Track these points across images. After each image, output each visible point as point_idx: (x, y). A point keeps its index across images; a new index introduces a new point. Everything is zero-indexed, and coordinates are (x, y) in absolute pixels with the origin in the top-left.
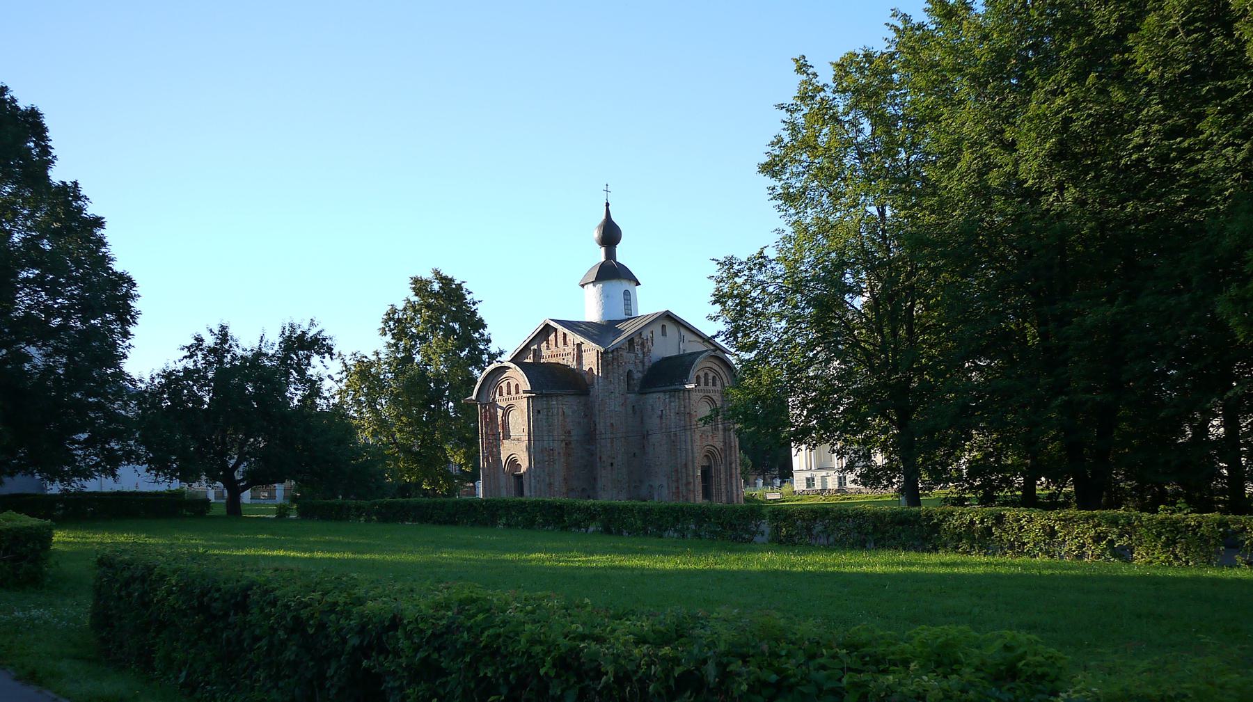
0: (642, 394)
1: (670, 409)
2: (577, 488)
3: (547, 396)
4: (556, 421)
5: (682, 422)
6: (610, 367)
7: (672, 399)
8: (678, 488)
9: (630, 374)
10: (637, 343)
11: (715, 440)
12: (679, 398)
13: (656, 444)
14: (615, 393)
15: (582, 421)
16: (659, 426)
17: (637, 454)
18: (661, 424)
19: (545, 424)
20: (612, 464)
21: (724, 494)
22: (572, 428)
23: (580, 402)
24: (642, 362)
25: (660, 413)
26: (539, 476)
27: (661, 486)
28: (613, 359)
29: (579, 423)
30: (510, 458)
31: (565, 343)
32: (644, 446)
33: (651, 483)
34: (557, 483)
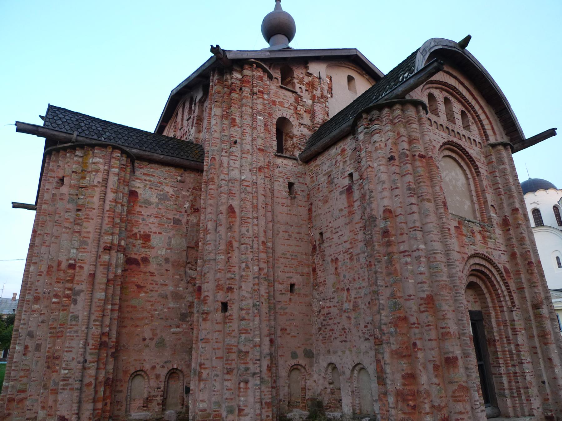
2: (154, 368)
4: (96, 199)
5: (409, 178)
6: (235, 95)
8: (411, 377)
9: (282, 123)
10: (301, 81)
11: (491, 243)
13: (340, 257)
14: (241, 144)
15: (184, 220)
16: (345, 212)
17: (296, 287)
21: (534, 391)
22: (154, 229)
23: (181, 182)
24: (312, 113)
25: (347, 182)
27: (359, 367)
29: (177, 222)
32: (314, 270)
33: (334, 359)
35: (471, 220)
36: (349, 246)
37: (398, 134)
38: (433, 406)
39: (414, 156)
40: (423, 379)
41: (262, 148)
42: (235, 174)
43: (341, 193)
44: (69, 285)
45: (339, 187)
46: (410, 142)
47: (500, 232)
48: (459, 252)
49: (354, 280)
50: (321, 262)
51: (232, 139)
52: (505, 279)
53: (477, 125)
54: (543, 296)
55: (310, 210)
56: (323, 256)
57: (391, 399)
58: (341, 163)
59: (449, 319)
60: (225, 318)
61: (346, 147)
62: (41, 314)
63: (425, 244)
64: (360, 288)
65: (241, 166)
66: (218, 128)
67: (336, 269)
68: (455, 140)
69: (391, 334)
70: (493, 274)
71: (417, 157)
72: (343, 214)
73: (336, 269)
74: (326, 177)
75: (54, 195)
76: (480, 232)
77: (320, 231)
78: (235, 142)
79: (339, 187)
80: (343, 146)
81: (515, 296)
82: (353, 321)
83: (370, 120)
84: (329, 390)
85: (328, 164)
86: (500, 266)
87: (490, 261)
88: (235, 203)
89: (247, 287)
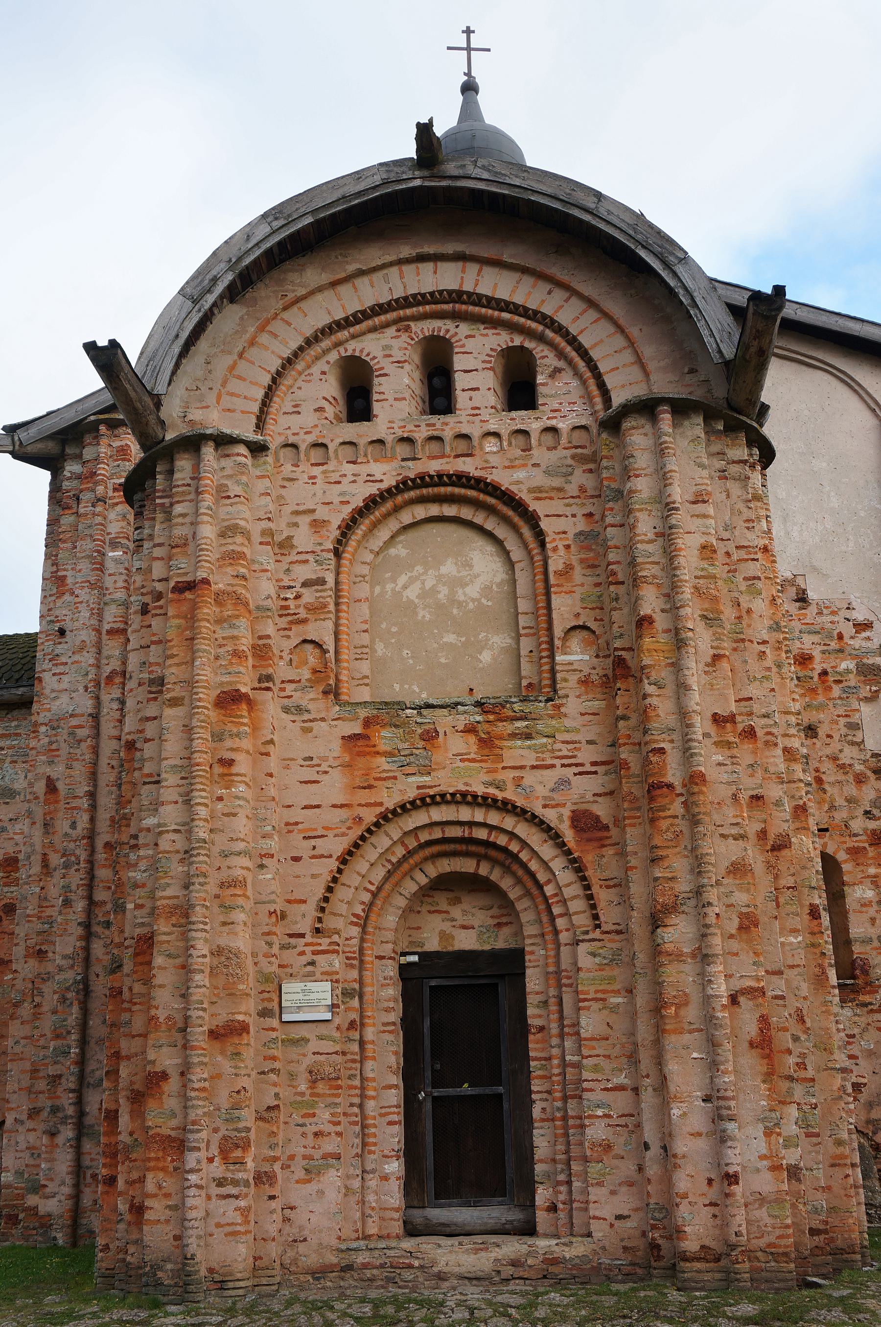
35: (431, 701)
41: (122, 626)
47: (596, 705)
48: (342, 806)
51: (56, 627)
52: (569, 852)
53: (577, 374)
54: (683, 886)
59: (160, 986)
68: (434, 467)
70: (524, 844)
76: (470, 729)
78: (62, 632)
81: (603, 896)
86: (550, 816)
87: (506, 807)
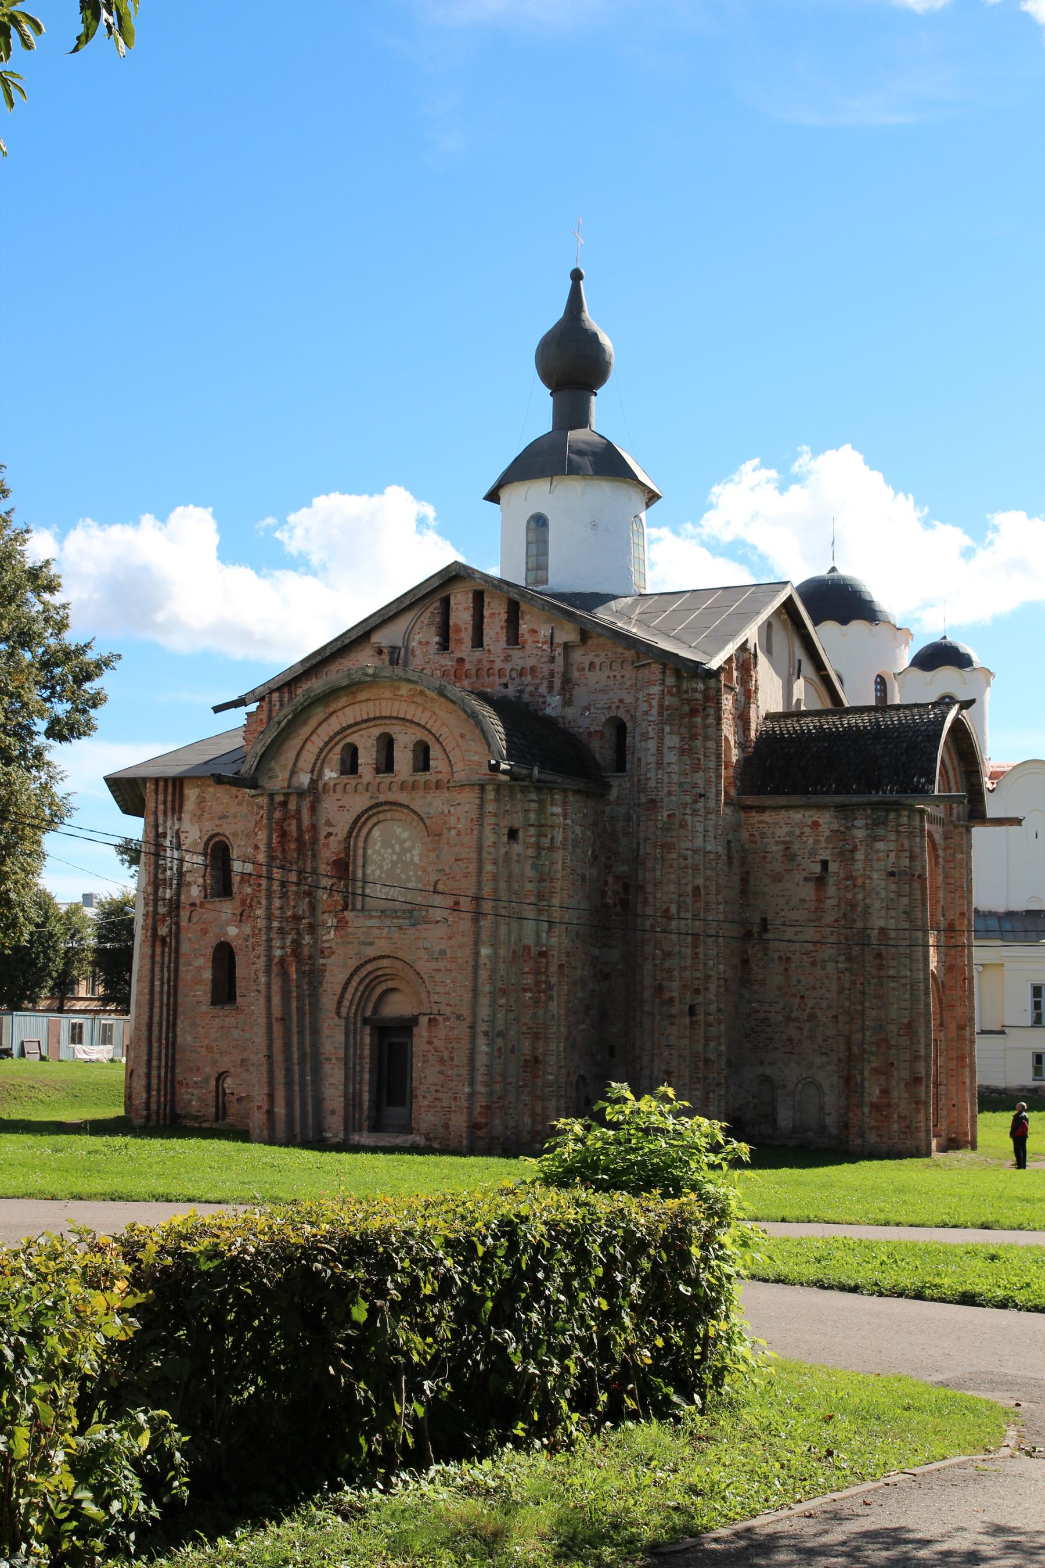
0: (747, 808)
1: (867, 859)
3: (540, 786)
4: (559, 867)
5: (905, 900)
7: (881, 832)
8: (885, 1092)
12: (898, 832)
13: (795, 958)
18: (820, 900)
19: (530, 873)
20: (692, 1011)
25: (817, 868)
26: (500, 1034)
28: (707, 698)
30: (369, 967)
31: (514, 638)
32: (745, 962)
34: (552, 1060)
36: (810, 947)
37: (902, 845)
38: (899, 1117)
39: (913, 875)
40: (895, 1094)
42: (699, 842)
43: (806, 879)
44: (544, 978)
45: (804, 870)
46: (912, 858)
49: (814, 988)
50: (759, 956)
51: (699, 791)
55: (744, 881)
56: (765, 950)
57: (866, 1110)
58: (810, 841)
60: (692, 1023)
61: (821, 822)
62: (511, 1011)
63: (911, 970)
64: (822, 999)
65: (706, 831)
66: (675, 768)
67: (786, 970)
69: (872, 1053)
71: (916, 878)
72: (806, 906)
73: (786, 970)
74: (781, 847)
75: (507, 853)
77: (764, 916)
79: (804, 870)
80: (815, 818)
82: (805, 1032)
83: (874, 820)
84: (752, 1105)
85: (786, 829)
88: (700, 882)
89: (713, 988)
